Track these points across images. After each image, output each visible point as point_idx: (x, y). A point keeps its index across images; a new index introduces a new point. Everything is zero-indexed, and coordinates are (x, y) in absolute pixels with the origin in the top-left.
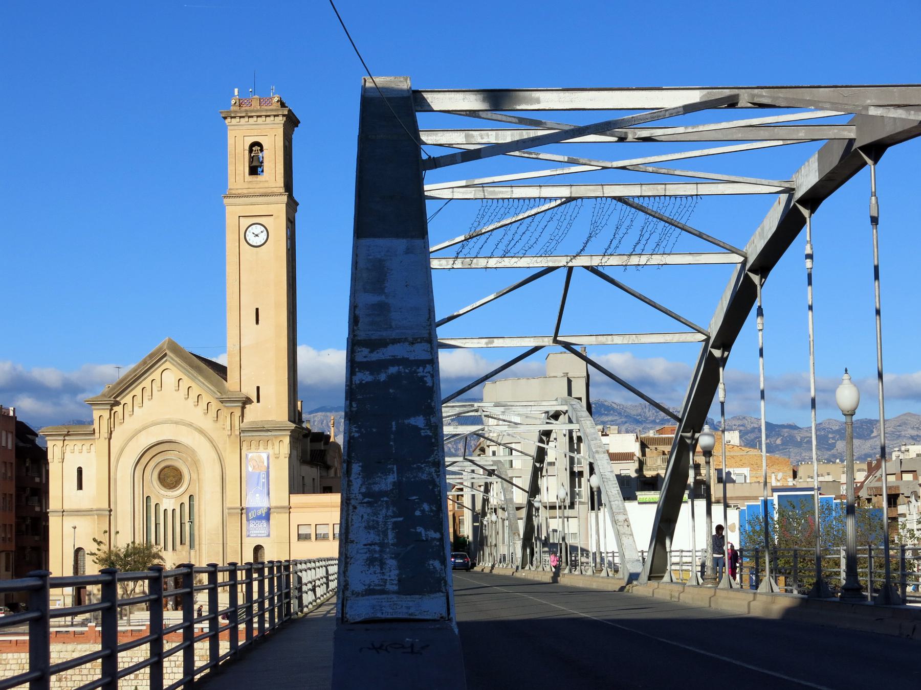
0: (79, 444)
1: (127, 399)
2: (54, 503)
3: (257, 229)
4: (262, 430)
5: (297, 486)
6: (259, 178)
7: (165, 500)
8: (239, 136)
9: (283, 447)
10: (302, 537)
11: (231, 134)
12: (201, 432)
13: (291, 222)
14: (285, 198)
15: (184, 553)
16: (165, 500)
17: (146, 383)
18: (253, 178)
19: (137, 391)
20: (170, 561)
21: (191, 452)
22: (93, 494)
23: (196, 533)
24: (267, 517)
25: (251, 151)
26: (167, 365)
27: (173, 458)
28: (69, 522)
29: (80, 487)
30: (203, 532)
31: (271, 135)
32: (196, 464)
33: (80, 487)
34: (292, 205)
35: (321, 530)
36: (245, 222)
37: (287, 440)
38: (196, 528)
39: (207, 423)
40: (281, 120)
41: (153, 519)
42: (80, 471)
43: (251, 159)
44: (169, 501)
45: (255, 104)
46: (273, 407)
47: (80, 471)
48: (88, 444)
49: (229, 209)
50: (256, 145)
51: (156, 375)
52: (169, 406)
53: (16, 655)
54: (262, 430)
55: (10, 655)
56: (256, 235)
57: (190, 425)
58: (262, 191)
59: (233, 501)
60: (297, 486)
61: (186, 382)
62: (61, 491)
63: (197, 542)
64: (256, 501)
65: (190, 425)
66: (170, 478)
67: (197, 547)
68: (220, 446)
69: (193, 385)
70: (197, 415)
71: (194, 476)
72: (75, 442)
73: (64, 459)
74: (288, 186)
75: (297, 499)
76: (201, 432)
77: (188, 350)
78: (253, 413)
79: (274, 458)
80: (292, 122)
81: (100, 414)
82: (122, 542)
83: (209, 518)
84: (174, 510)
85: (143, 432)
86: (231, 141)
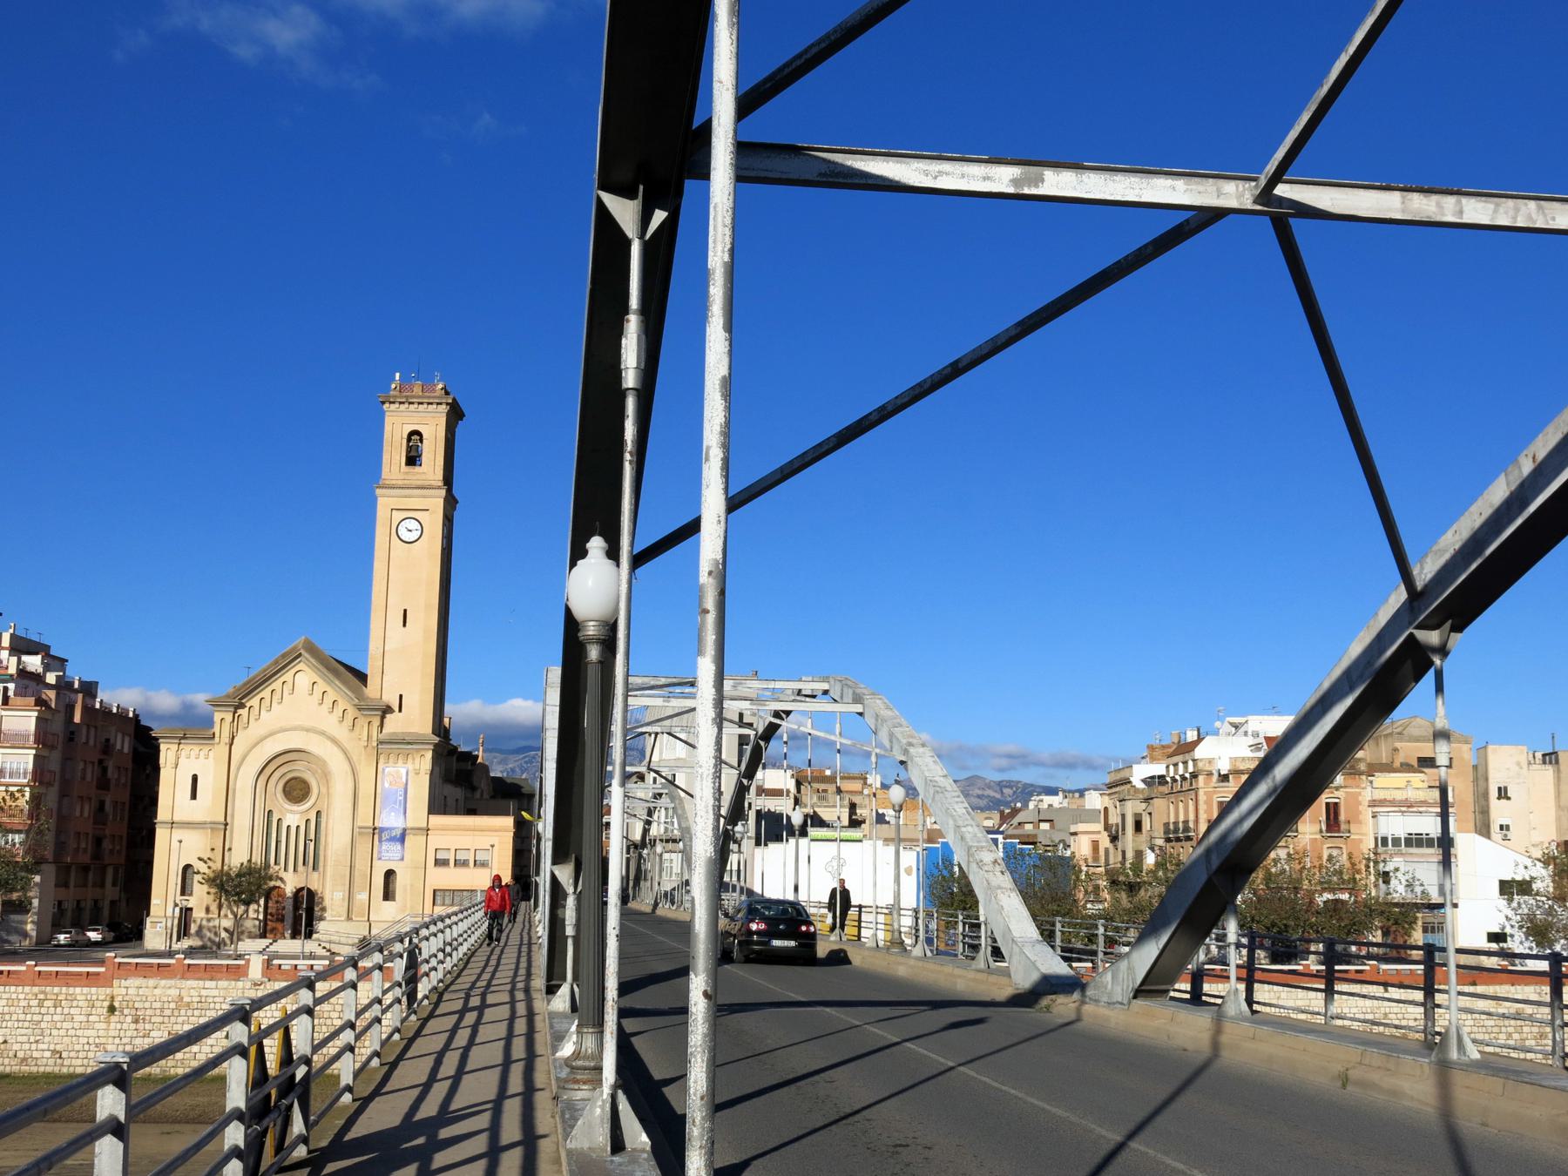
0: (196, 748)
1: (254, 702)
2: (163, 814)
3: (413, 525)
4: (403, 743)
5: (438, 805)
6: (417, 469)
8: (398, 423)
9: (425, 762)
10: (440, 863)
11: (388, 421)
12: (334, 741)
13: (448, 520)
14: (443, 492)
17: (277, 685)
18: (410, 469)
19: (266, 693)
20: (290, 883)
21: (322, 764)
22: (206, 807)
24: (402, 839)
25: (409, 440)
26: (301, 666)
27: (301, 770)
28: (178, 834)
29: (194, 796)
30: (329, 853)
31: (433, 424)
32: (326, 776)
33: (194, 796)
34: (451, 503)
35: (461, 856)
36: (398, 516)
37: (429, 755)
39: (341, 732)
40: (444, 409)
42: (195, 779)
43: (409, 449)
44: (293, 816)
45: (417, 390)
46: (416, 718)
47: (195, 779)
48: (206, 749)
49: (381, 501)
50: (415, 434)
51: (288, 676)
52: (300, 710)
53: (86, 990)
54: (403, 743)
55: (78, 990)
56: (409, 530)
57: (323, 733)
58: (419, 483)
59: (365, 819)
60: (438, 805)
61: (322, 686)
62: (172, 798)
64: (391, 820)
65: (323, 733)
66: (296, 791)
68: (355, 758)
69: (328, 689)
70: (331, 723)
71: (324, 790)
73: (177, 764)
74: (448, 480)
75: (437, 820)
76: (334, 741)
77: (327, 653)
78: (394, 724)
79: (413, 775)
80: (455, 414)
81: (222, 717)
82: (238, 858)
83: (337, 837)
86: (388, 428)
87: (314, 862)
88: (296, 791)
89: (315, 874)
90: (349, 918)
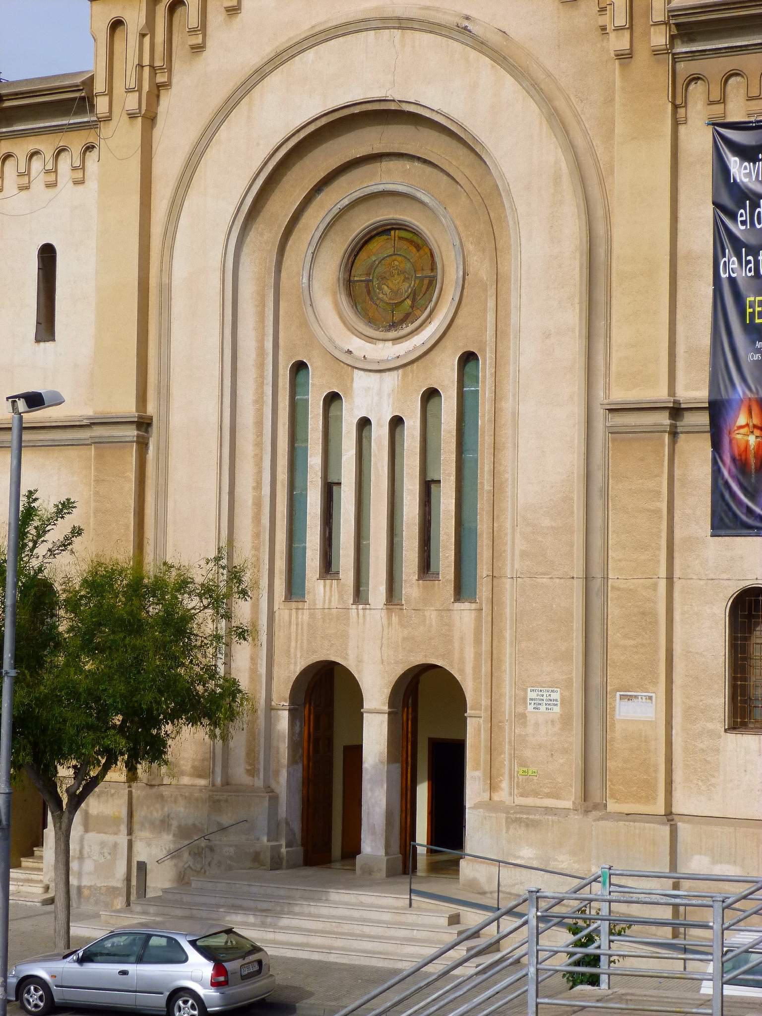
0: (46, 146)
7: (361, 380)
15: (431, 615)
16: (361, 380)
23: (483, 526)
38: (483, 504)
41: (315, 460)
42: (47, 255)
47: (47, 255)
57: (462, 32)
63: (483, 570)
65: (462, 32)
66: (390, 276)
67: (483, 591)
71: (481, 268)
72: (31, 144)
76: (501, 54)
84: (397, 422)
85: (275, 79)
87: (451, 550)
88: (390, 276)
89: (464, 615)
90: (589, 802)
